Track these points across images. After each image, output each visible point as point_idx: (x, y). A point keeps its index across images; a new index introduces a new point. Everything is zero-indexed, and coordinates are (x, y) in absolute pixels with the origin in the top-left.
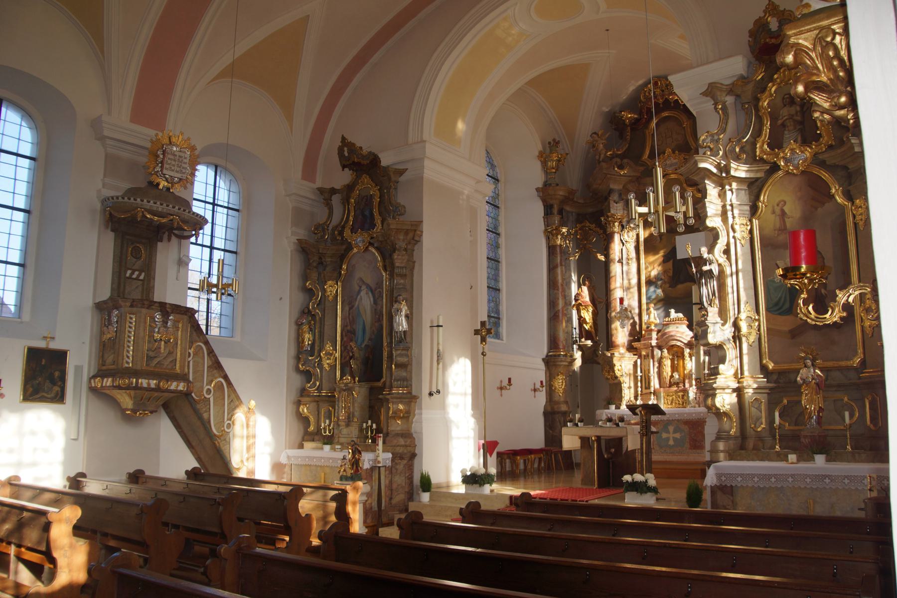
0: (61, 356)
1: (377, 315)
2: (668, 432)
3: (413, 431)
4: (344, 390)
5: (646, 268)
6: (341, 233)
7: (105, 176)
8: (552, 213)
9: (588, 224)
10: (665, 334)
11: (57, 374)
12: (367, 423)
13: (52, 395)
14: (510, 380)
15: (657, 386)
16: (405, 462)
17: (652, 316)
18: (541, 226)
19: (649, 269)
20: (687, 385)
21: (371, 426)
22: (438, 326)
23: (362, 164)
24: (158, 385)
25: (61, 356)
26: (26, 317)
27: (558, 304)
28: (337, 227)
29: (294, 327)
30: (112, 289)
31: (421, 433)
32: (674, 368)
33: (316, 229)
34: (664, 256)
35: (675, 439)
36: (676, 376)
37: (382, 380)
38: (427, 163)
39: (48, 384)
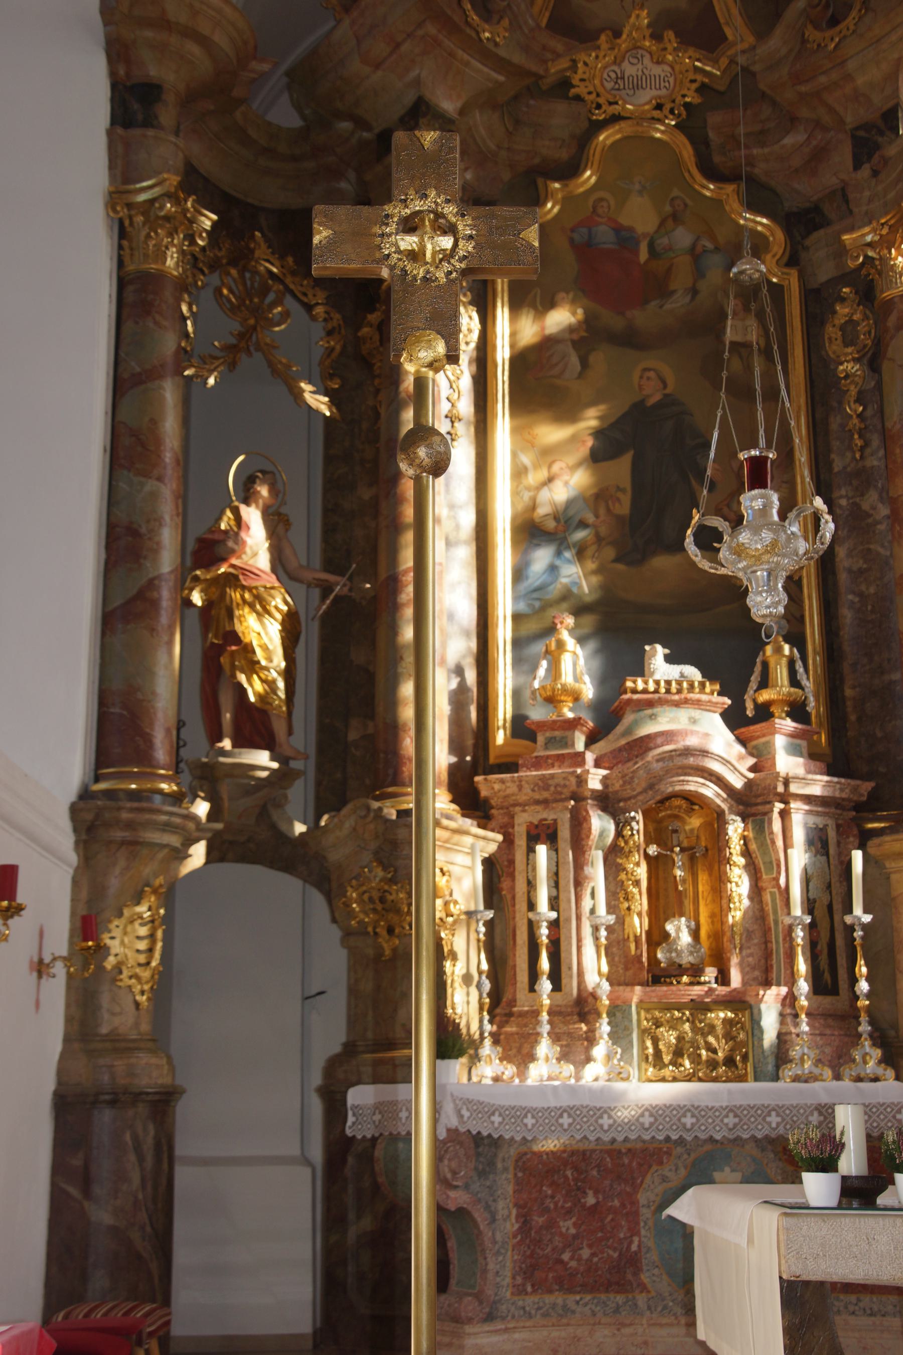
5: (519, 473)
8: (149, 122)
9: (262, 250)
10: (644, 744)
19: (533, 478)
20: (736, 979)
27: (156, 550)
34: (598, 434)
36: (680, 931)
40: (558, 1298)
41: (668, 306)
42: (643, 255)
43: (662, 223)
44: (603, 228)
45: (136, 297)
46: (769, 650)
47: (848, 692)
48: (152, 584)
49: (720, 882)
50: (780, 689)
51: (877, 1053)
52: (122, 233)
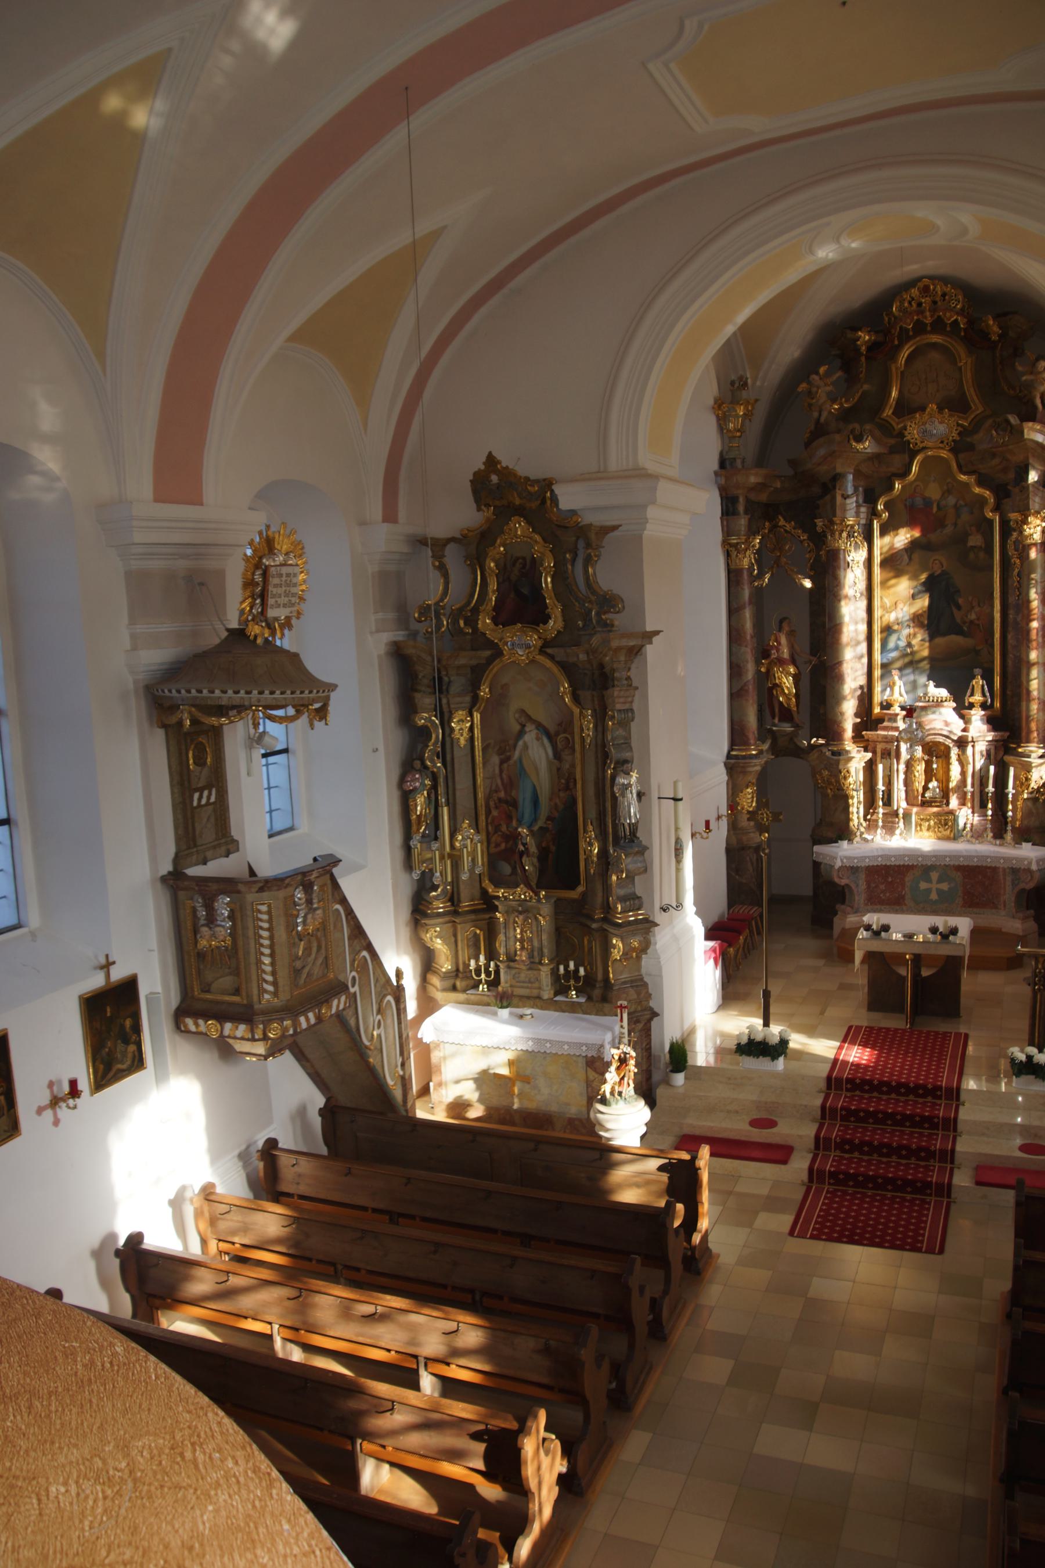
0: (125, 993)
1: (565, 782)
2: (929, 881)
3: (643, 971)
4: (520, 913)
6: (471, 622)
7: (132, 621)
9: (782, 522)
11: (128, 1023)
12: (566, 967)
13: (129, 1062)
14: (707, 823)
15: (904, 804)
16: (640, 1026)
17: (896, 689)
18: (719, 536)
21: (577, 971)
22: (676, 800)
23: (505, 493)
24: (319, 1019)
25: (130, 986)
26: (34, 919)
28: (461, 610)
29: (396, 794)
30: (178, 840)
31: (660, 976)
32: (929, 774)
33: (421, 614)
35: (940, 892)
37: (581, 889)
38: (651, 512)
39: (120, 1047)
40: (879, 907)
41: (945, 532)
42: (935, 509)
43: (943, 495)
44: (918, 499)
45: (733, 577)
46: (974, 682)
47: (1008, 693)
48: (745, 684)
49: (947, 770)
50: (977, 698)
51: (991, 835)
52: (728, 555)
